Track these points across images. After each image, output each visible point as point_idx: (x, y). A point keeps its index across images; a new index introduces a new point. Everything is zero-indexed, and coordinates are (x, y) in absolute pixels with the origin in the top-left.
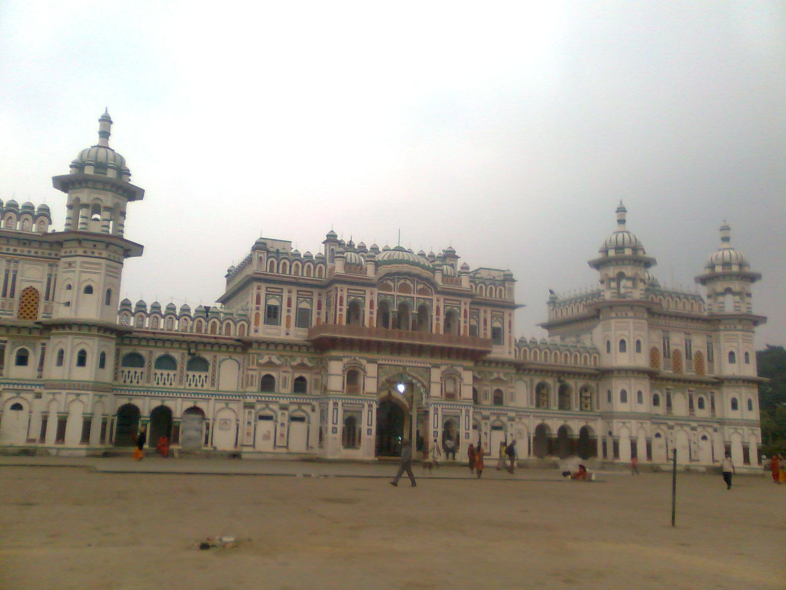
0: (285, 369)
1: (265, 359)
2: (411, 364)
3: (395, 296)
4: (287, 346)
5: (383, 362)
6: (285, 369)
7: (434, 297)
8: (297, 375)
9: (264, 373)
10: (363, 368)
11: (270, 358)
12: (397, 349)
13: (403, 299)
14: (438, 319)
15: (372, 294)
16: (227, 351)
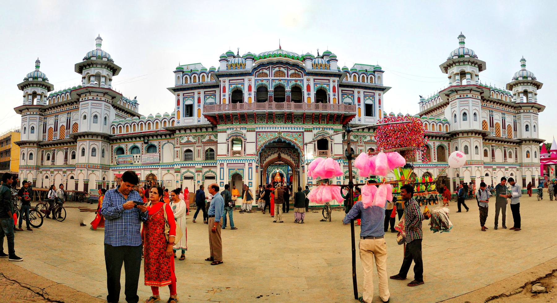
0: (198, 144)
1: (185, 140)
2: (285, 130)
3: (271, 82)
4: (197, 128)
5: (261, 130)
6: (198, 144)
7: (305, 78)
8: (207, 148)
9: (185, 149)
10: (243, 136)
11: (188, 139)
12: (270, 118)
13: (277, 82)
14: (309, 94)
15: (250, 80)
16: (166, 138)
